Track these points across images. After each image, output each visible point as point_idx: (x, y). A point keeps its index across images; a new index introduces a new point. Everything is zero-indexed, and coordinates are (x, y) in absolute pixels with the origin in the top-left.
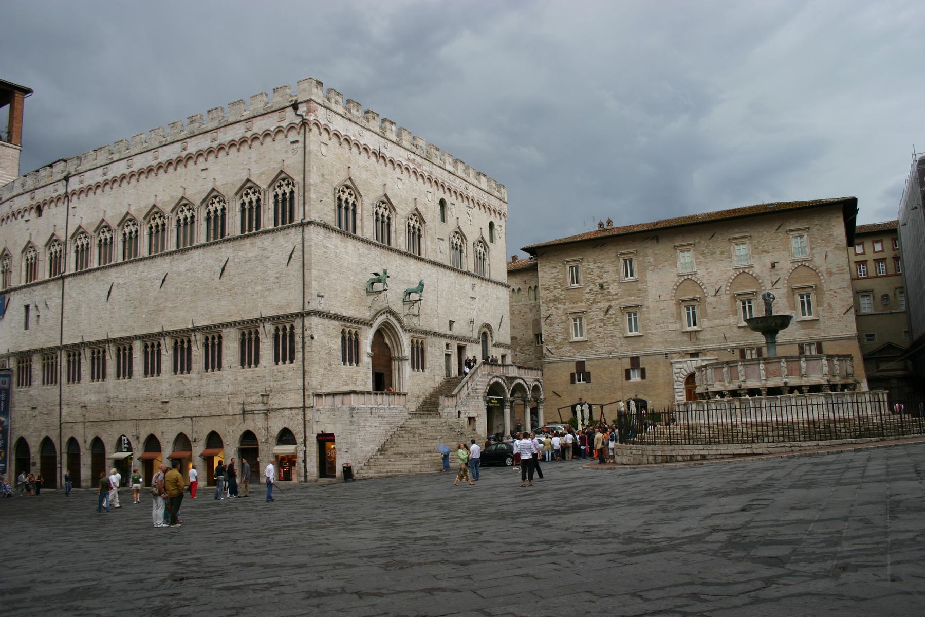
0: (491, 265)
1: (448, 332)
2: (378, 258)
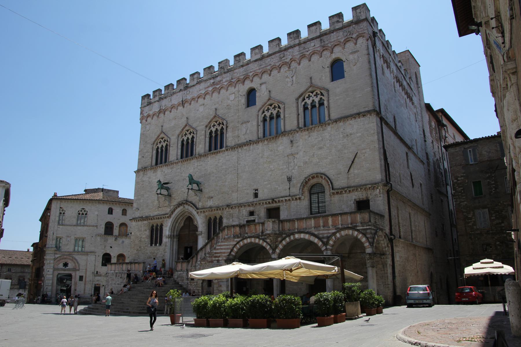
0: (332, 105)
1: (251, 199)
2: (179, 170)
